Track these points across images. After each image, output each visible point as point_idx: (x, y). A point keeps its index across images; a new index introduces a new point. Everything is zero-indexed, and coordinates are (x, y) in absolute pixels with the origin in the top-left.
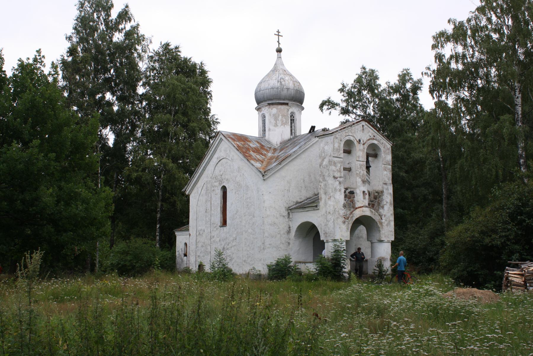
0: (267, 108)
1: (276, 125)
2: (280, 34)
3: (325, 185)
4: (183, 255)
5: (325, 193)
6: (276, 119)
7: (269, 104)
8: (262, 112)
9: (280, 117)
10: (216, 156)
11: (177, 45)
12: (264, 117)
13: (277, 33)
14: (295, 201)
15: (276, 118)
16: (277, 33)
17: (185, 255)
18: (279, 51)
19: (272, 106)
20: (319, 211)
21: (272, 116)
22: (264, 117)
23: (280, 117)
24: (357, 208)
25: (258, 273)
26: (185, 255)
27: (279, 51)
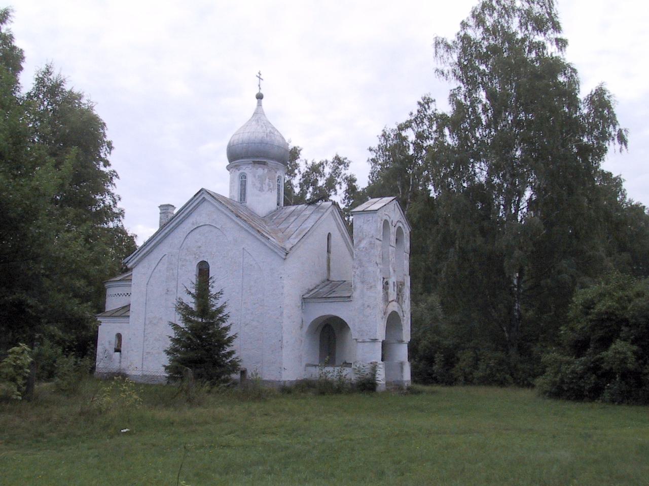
0: (250, 166)
1: (261, 190)
2: (261, 77)
3: (363, 273)
4: (112, 351)
5: (363, 282)
6: (262, 183)
7: (254, 162)
8: (241, 171)
9: (267, 180)
10: (191, 220)
11: (368, 151)
12: (243, 178)
13: (258, 75)
14: (307, 288)
15: (261, 180)
16: (258, 75)
17: (118, 350)
18: (260, 97)
19: (257, 165)
20: (352, 302)
21: (257, 177)
22: (243, 178)
23: (267, 180)
24: (390, 302)
25: (573, 341)
26: (118, 350)
27: (260, 97)
